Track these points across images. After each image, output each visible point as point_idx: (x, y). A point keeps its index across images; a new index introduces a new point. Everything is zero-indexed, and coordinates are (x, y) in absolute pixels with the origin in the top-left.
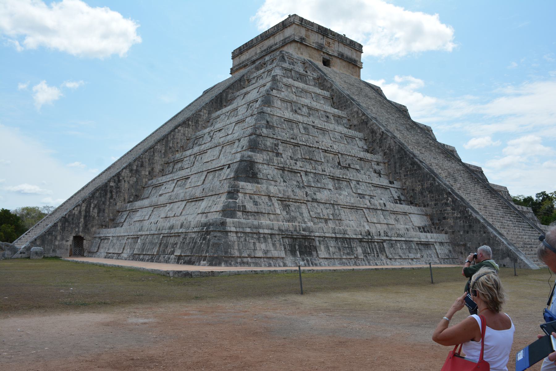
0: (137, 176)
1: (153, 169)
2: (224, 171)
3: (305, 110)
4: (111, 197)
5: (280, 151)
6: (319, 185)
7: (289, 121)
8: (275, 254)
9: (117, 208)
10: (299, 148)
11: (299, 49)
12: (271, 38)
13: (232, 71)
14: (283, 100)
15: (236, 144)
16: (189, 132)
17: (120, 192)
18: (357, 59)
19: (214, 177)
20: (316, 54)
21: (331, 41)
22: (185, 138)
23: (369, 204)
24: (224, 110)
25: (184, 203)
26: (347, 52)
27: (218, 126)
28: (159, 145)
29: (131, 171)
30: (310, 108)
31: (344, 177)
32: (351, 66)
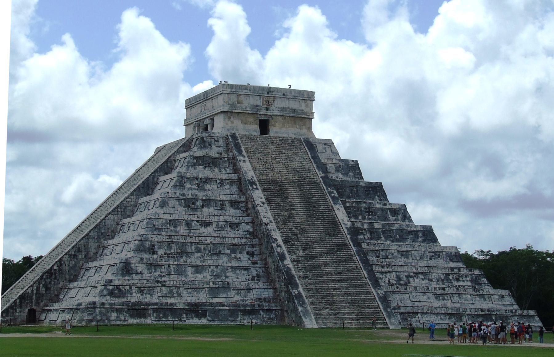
0: (75, 260)
1: (88, 253)
3: (199, 203)
4: (55, 278)
5: (156, 250)
7: (176, 221)
8: (123, 318)
9: (60, 286)
10: (173, 245)
11: (230, 118)
12: (210, 100)
14: (178, 199)
16: (117, 217)
17: (62, 273)
20: (251, 119)
22: (115, 223)
23: (211, 283)
26: (293, 105)
28: (92, 232)
31: (204, 264)
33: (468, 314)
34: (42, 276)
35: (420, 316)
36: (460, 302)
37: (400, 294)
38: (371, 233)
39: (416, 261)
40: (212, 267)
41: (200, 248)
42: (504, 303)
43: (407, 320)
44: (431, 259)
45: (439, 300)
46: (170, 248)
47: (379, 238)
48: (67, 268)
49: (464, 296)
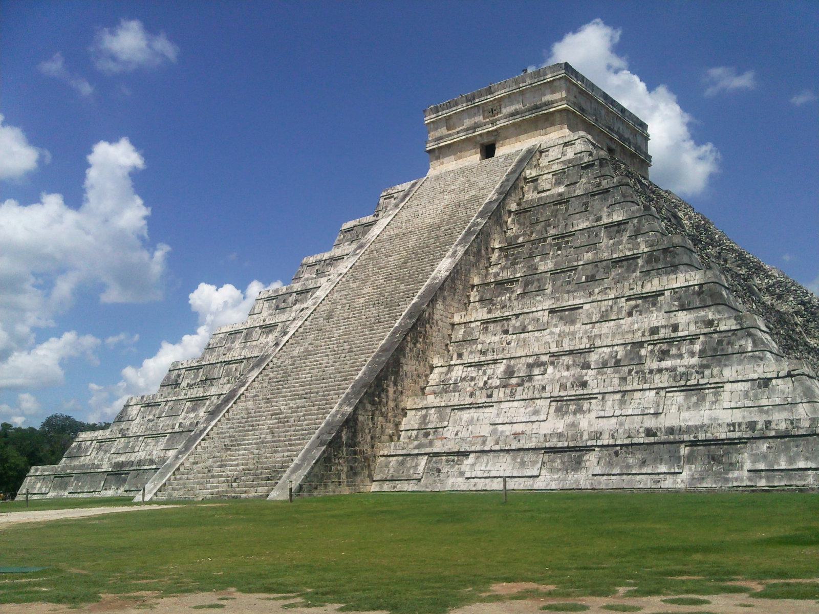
5: (180, 381)
31: (205, 395)
33: (603, 446)
35: (472, 459)
36: (617, 413)
37: (473, 411)
38: (526, 285)
39: (589, 326)
40: (213, 398)
41: (231, 369)
42: (764, 402)
43: (439, 471)
44: (630, 314)
45: (567, 412)
46: (196, 376)
47: (541, 290)
49: (637, 395)
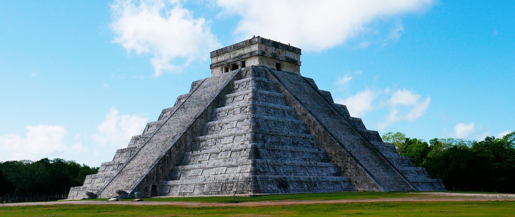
2: (243, 151)
3: (272, 110)
4: (168, 163)
6: (285, 156)
8: (274, 188)
11: (262, 60)
13: (212, 67)
14: (261, 107)
15: (244, 136)
16: (203, 121)
18: (298, 60)
19: (237, 154)
21: (281, 50)
24: (223, 108)
25: (226, 167)
26: (291, 55)
27: (225, 120)
29: (176, 147)
30: (275, 109)
32: (294, 65)
34: (159, 162)
40: (301, 153)
48: (174, 156)
